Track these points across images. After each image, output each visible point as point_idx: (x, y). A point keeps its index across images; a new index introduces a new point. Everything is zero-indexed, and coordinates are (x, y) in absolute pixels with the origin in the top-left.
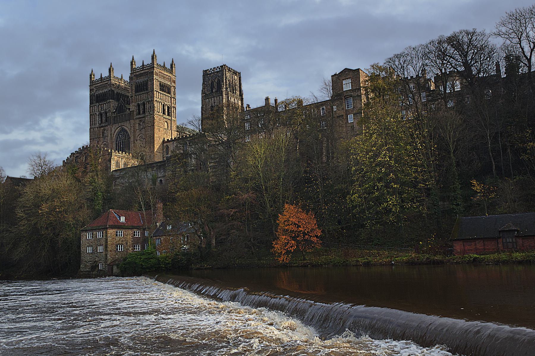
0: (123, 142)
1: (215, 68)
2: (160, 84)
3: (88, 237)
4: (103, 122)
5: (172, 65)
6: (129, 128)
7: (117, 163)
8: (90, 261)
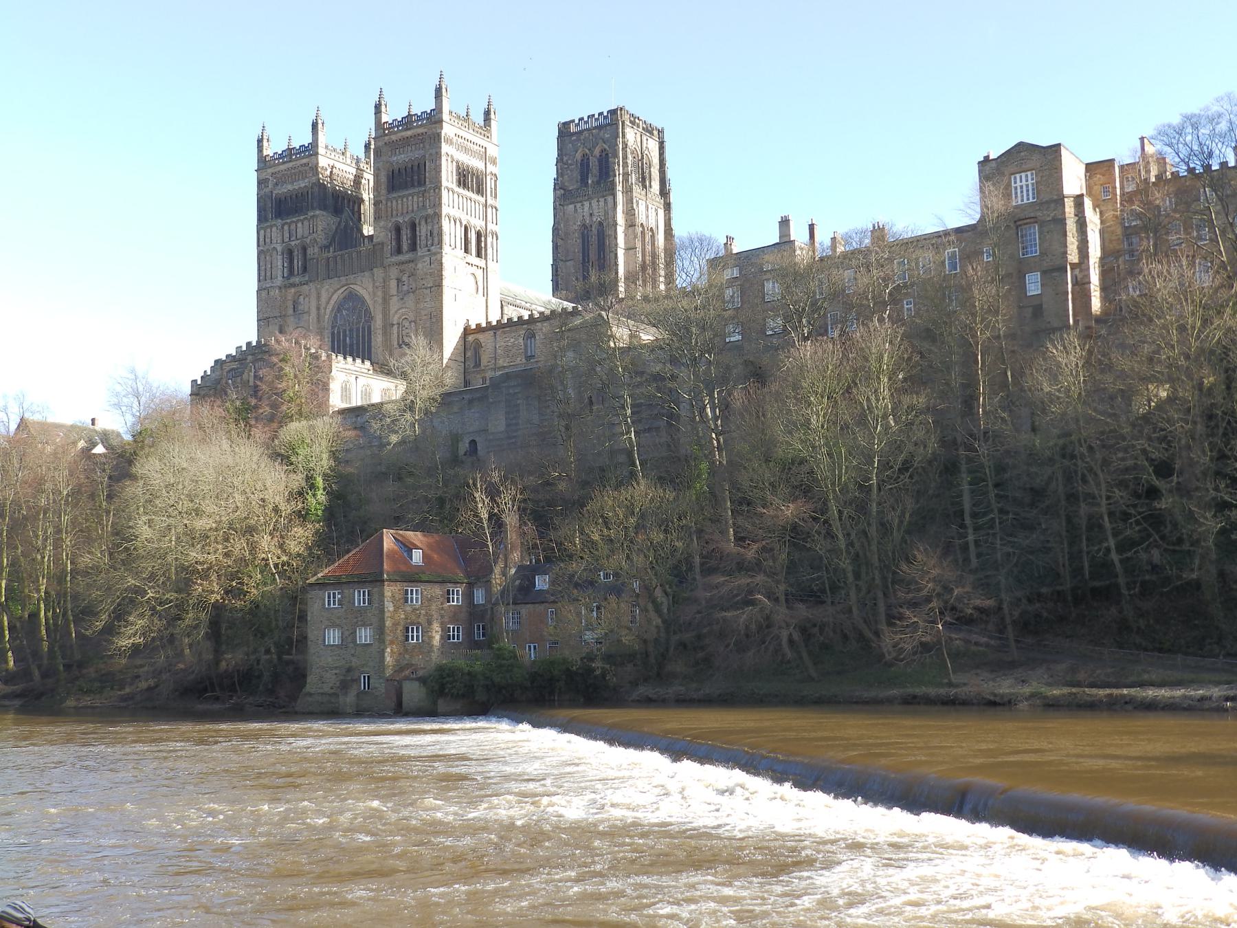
0: (351, 330)
1: (593, 115)
2: (458, 167)
3: (329, 601)
4: (296, 272)
5: (487, 114)
6: (371, 289)
7: (345, 391)
8: (336, 668)
